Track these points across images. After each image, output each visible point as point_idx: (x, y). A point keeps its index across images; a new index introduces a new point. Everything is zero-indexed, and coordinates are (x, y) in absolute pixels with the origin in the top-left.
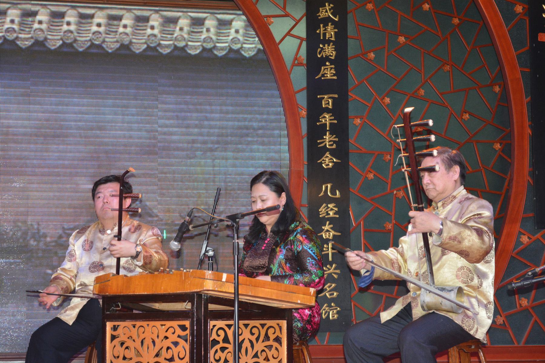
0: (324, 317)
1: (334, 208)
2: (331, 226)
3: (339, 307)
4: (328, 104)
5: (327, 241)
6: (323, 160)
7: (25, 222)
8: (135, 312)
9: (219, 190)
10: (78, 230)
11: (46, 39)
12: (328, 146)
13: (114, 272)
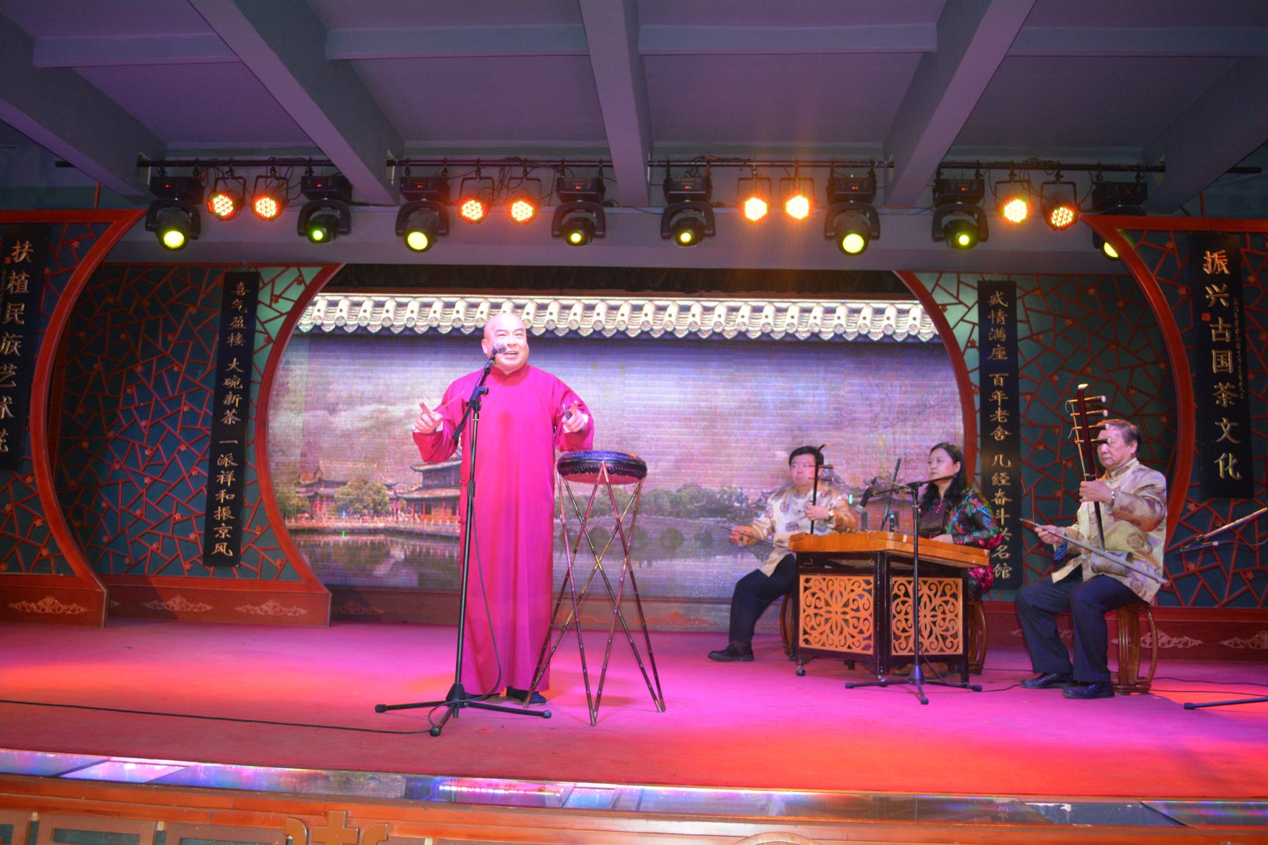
0: (997, 575)
2: (1003, 493)
5: (999, 507)
7: (730, 487)
8: (826, 567)
9: (899, 461)
11: (747, 331)
13: (809, 532)
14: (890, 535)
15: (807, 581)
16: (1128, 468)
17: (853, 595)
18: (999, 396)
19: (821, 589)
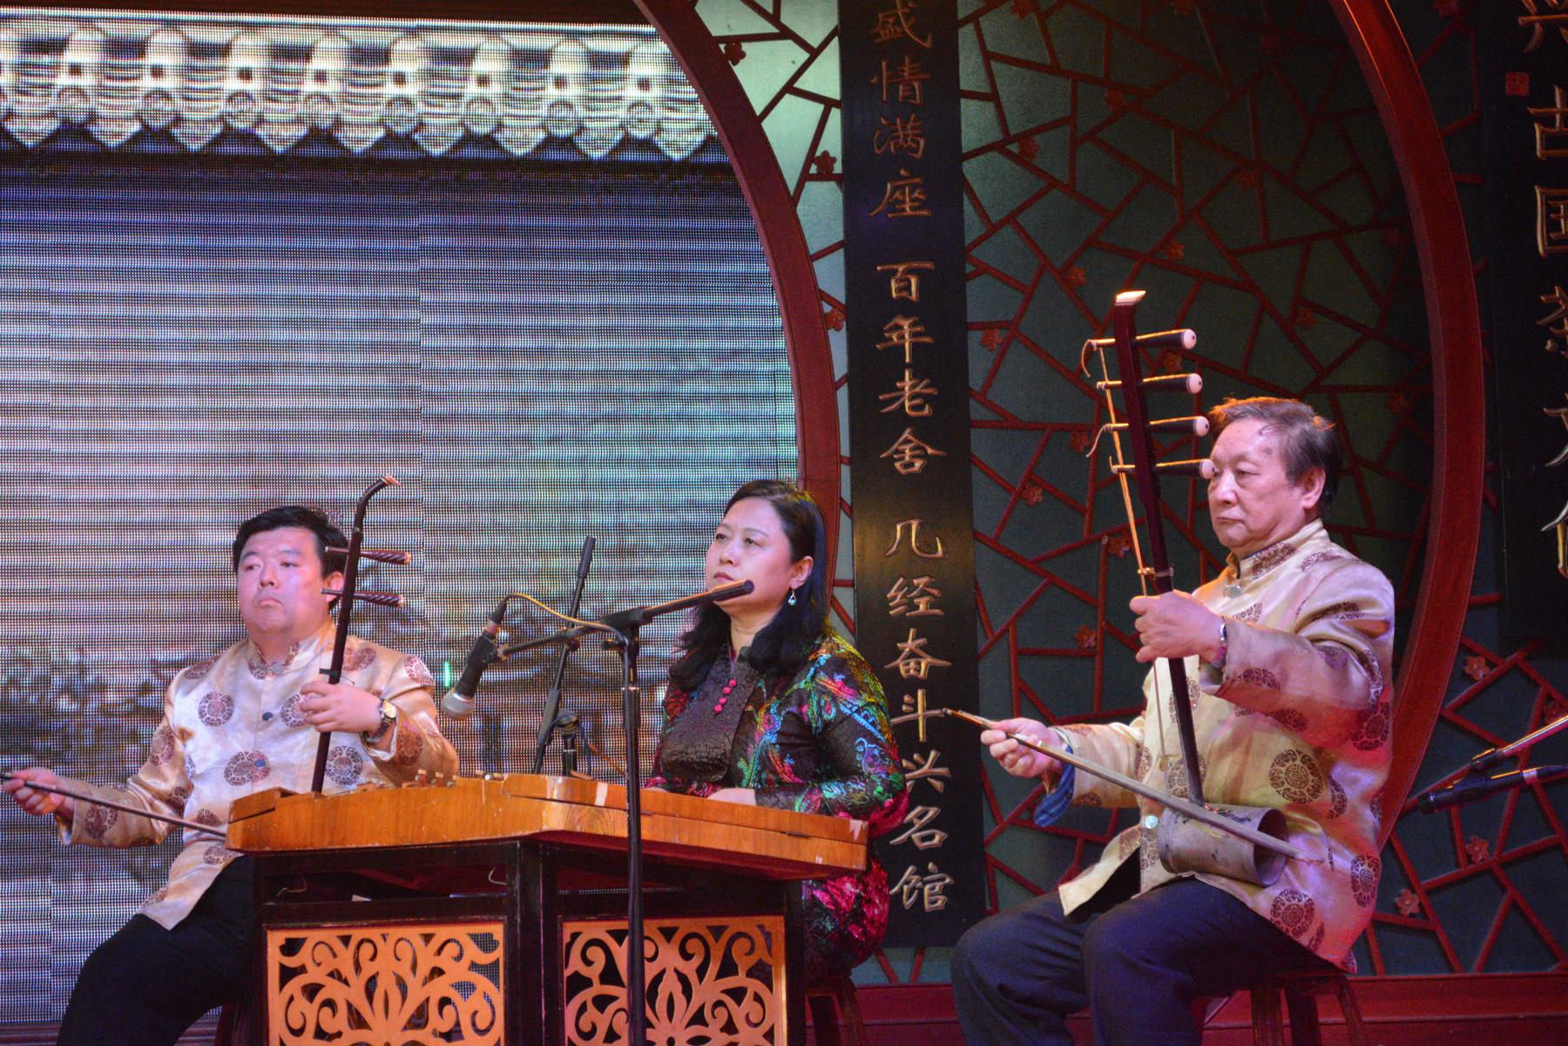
0: (908, 903)
1: (929, 590)
3: (950, 875)
4: (908, 288)
5: (912, 685)
6: (897, 451)
8: (356, 898)
10: (187, 669)
12: (907, 410)
14: (555, 784)
15: (290, 948)
16: (1291, 550)
17: (440, 987)
18: (905, 334)
19: (335, 975)
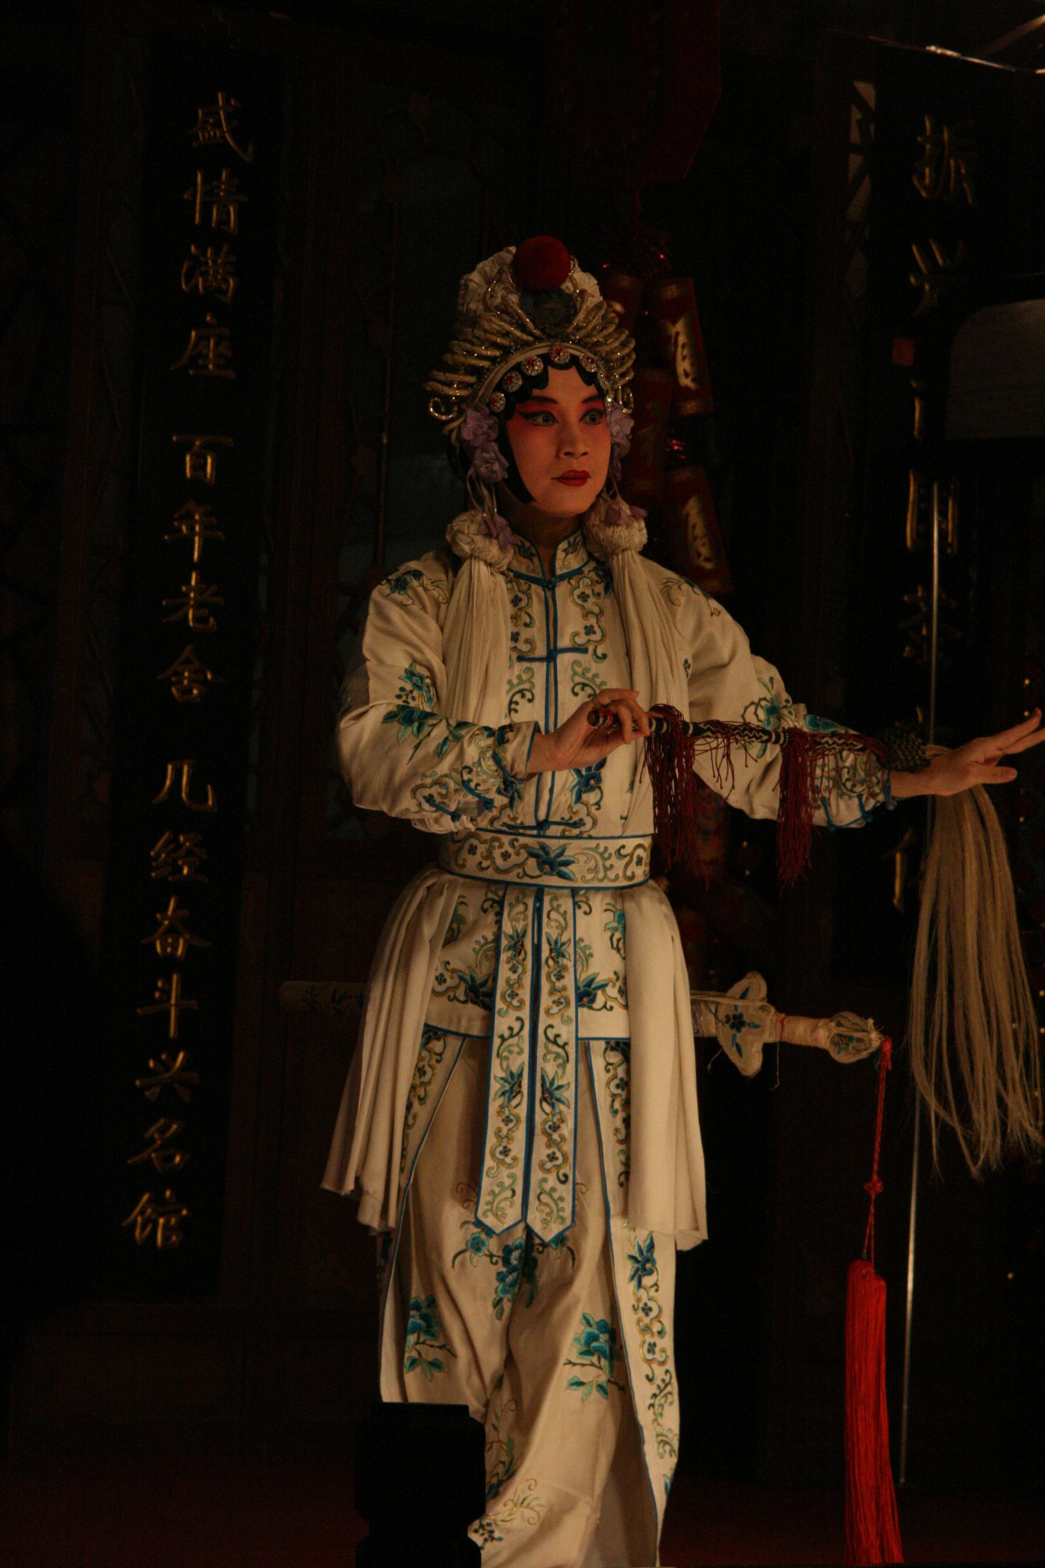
5: (168, 965)
6: (175, 674)
